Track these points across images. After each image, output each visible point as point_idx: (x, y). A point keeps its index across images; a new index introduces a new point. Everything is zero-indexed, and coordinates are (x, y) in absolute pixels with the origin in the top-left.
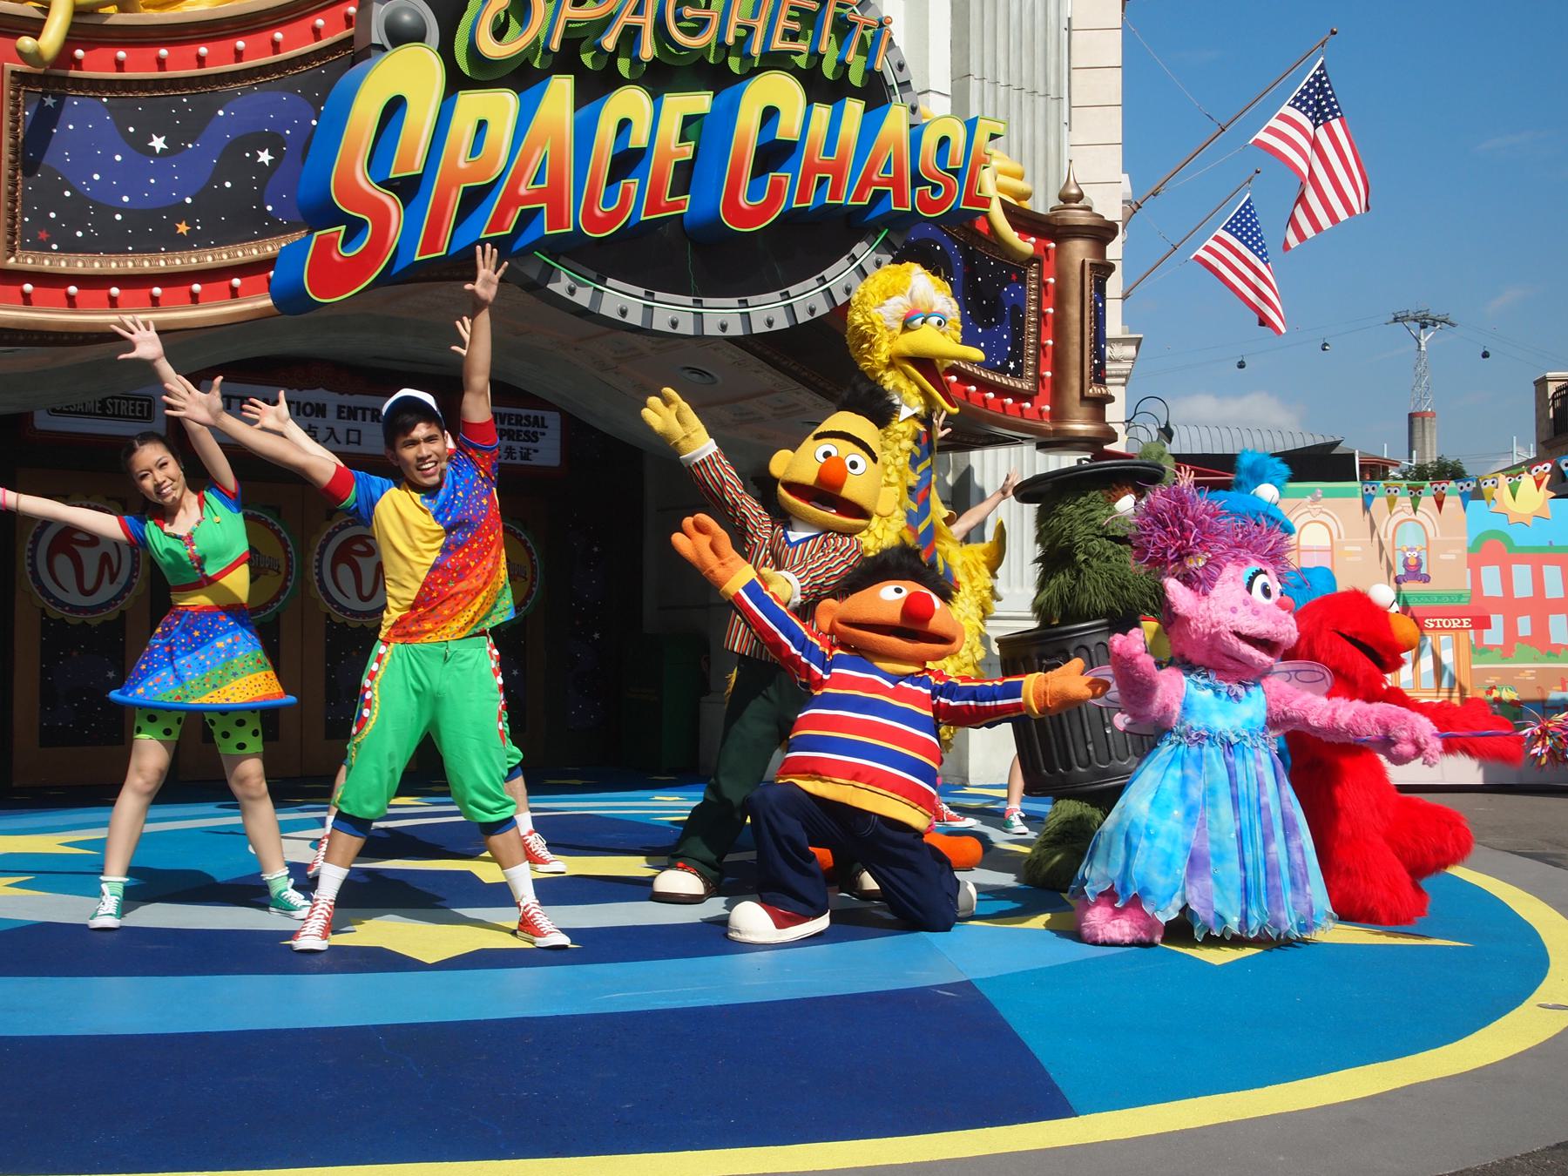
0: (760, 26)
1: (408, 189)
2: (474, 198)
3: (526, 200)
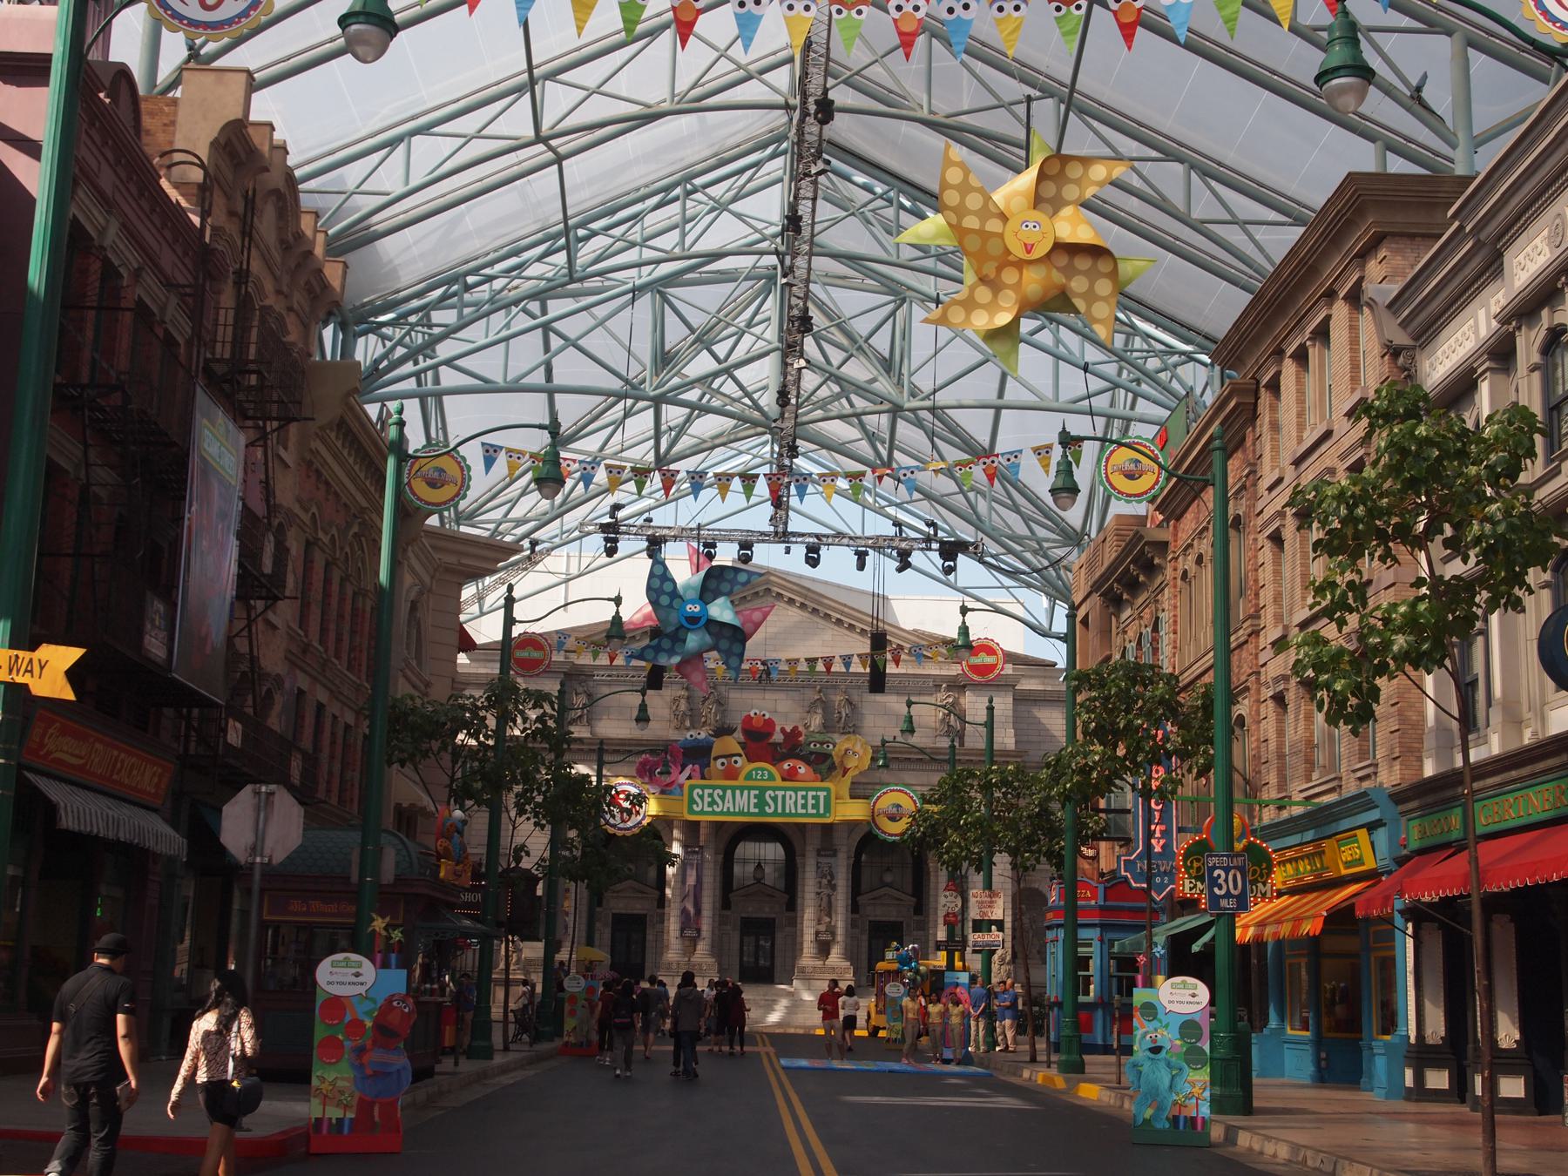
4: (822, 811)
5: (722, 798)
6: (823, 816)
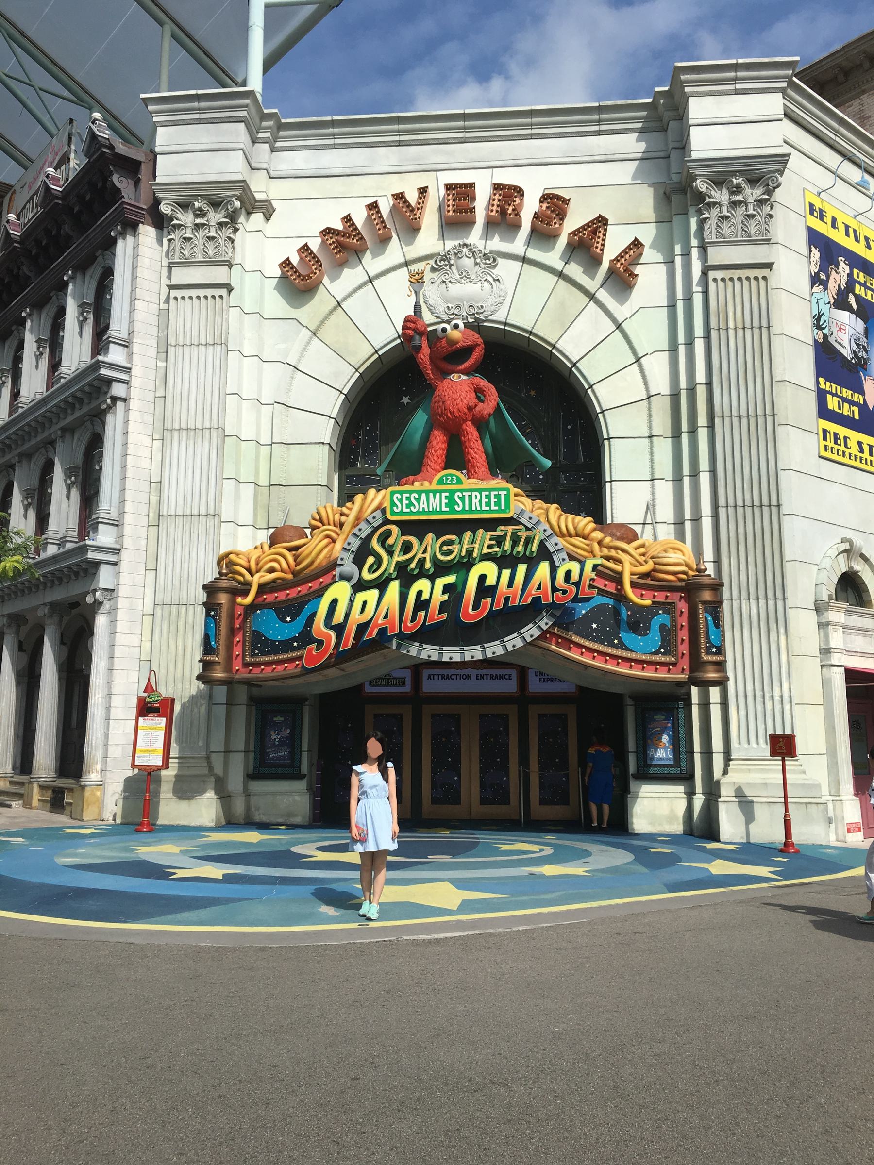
0: (476, 546)
1: (340, 629)
2: (362, 628)
3: (381, 624)
4: (503, 508)
5: (418, 500)
6: (503, 511)
